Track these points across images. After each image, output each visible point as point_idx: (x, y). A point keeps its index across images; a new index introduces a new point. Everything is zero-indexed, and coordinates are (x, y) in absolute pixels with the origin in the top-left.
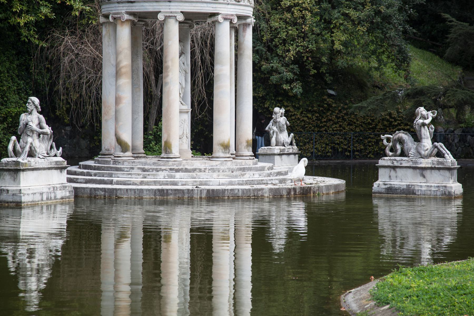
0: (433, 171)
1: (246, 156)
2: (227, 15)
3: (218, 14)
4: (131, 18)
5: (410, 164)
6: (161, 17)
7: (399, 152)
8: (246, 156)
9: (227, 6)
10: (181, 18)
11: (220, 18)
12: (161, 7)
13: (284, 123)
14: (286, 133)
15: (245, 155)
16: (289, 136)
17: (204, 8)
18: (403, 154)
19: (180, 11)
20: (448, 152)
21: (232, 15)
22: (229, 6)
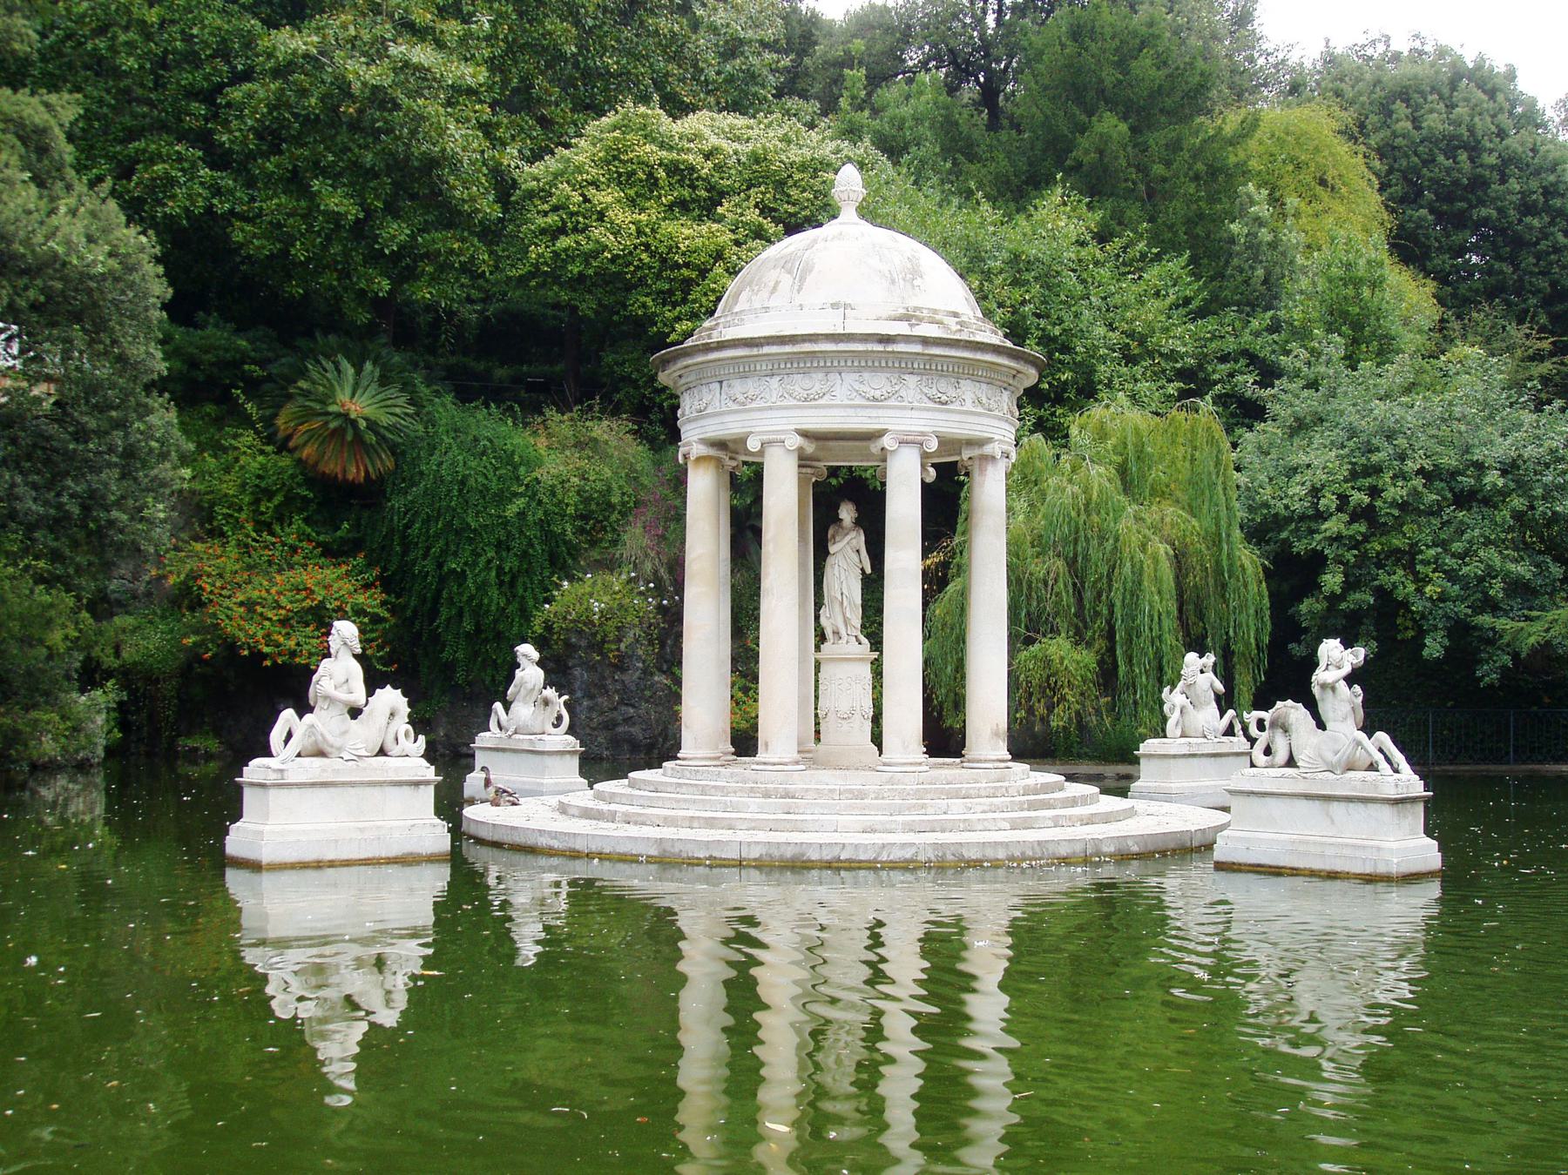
0: (1351, 805)
1: (986, 761)
2: (908, 433)
3: (879, 434)
4: (712, 452)
5: (1301, 788)
6: (753, 445)
7: (1281, 755)
8: (986, 761)
9: (909, 413)
10: (796, 441)
11: (887, 442)
12: (754, 423)
13: (1206, 686)
14: (1213, 708)
15: (982, 758)
16: (1222, 714)
17: (848, 420)
18: (1291, 762)
19: (793, 427)
20: (1399, 758)
21: (923, 434)
22: (915, 414)
